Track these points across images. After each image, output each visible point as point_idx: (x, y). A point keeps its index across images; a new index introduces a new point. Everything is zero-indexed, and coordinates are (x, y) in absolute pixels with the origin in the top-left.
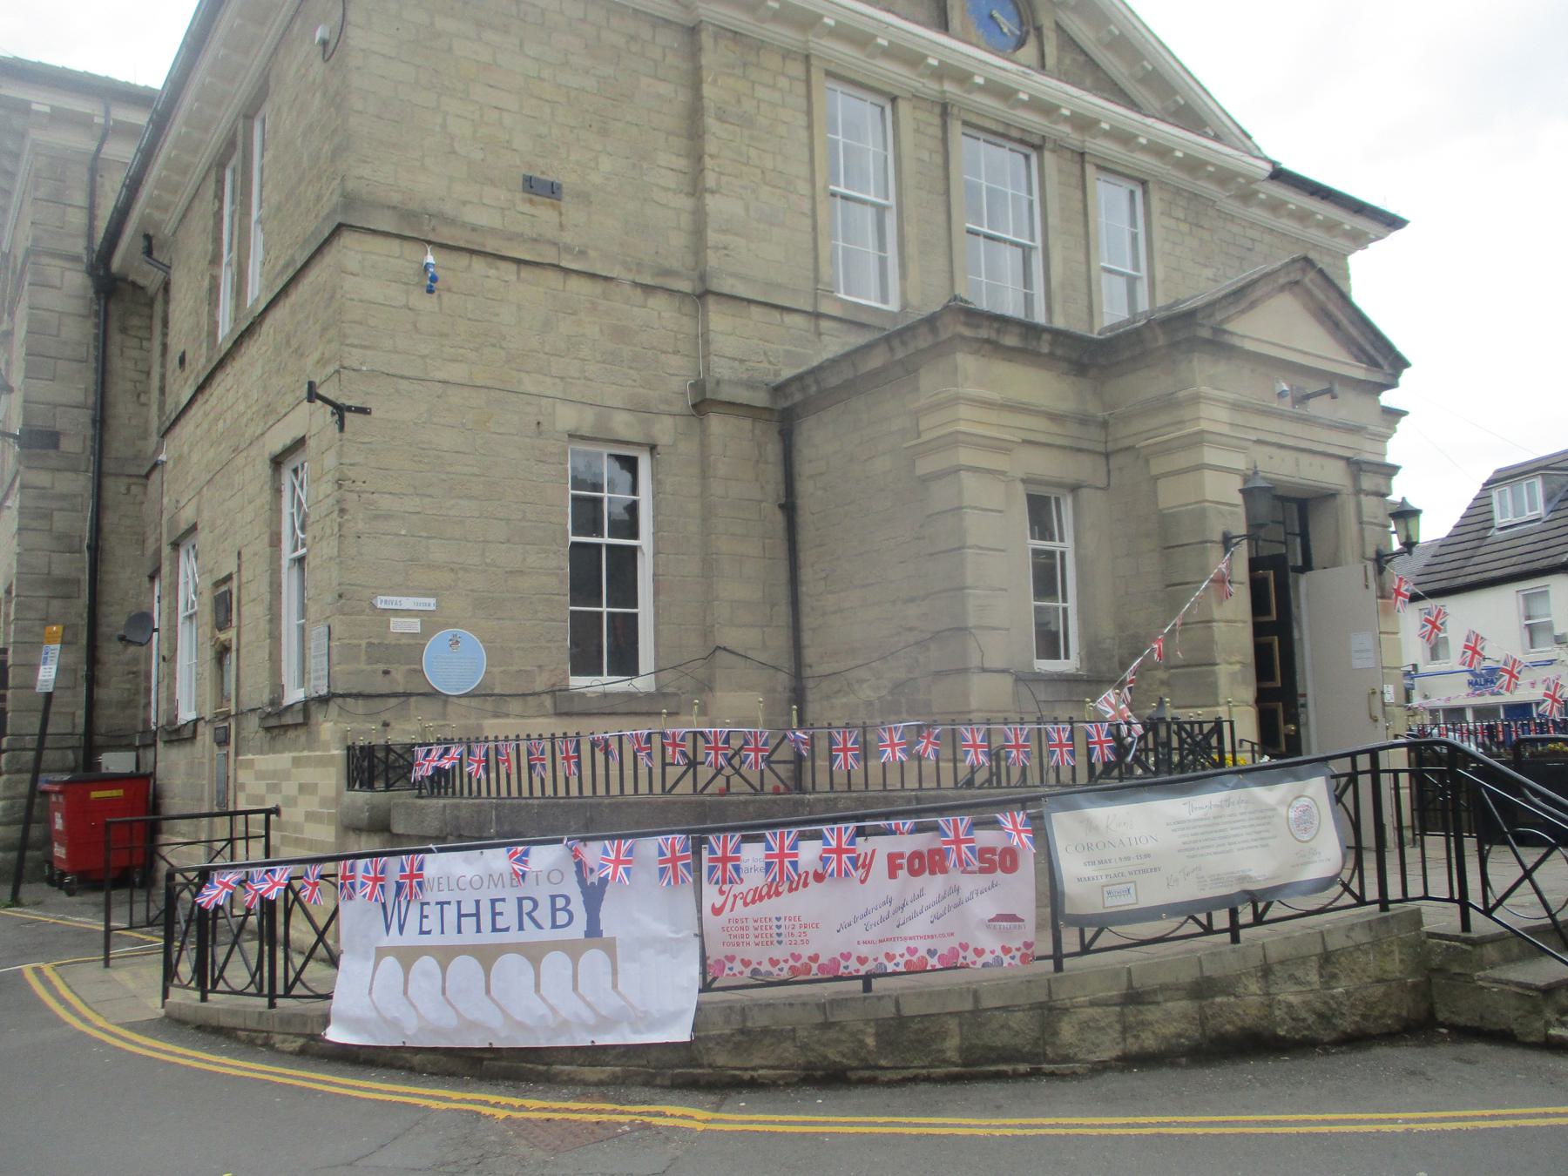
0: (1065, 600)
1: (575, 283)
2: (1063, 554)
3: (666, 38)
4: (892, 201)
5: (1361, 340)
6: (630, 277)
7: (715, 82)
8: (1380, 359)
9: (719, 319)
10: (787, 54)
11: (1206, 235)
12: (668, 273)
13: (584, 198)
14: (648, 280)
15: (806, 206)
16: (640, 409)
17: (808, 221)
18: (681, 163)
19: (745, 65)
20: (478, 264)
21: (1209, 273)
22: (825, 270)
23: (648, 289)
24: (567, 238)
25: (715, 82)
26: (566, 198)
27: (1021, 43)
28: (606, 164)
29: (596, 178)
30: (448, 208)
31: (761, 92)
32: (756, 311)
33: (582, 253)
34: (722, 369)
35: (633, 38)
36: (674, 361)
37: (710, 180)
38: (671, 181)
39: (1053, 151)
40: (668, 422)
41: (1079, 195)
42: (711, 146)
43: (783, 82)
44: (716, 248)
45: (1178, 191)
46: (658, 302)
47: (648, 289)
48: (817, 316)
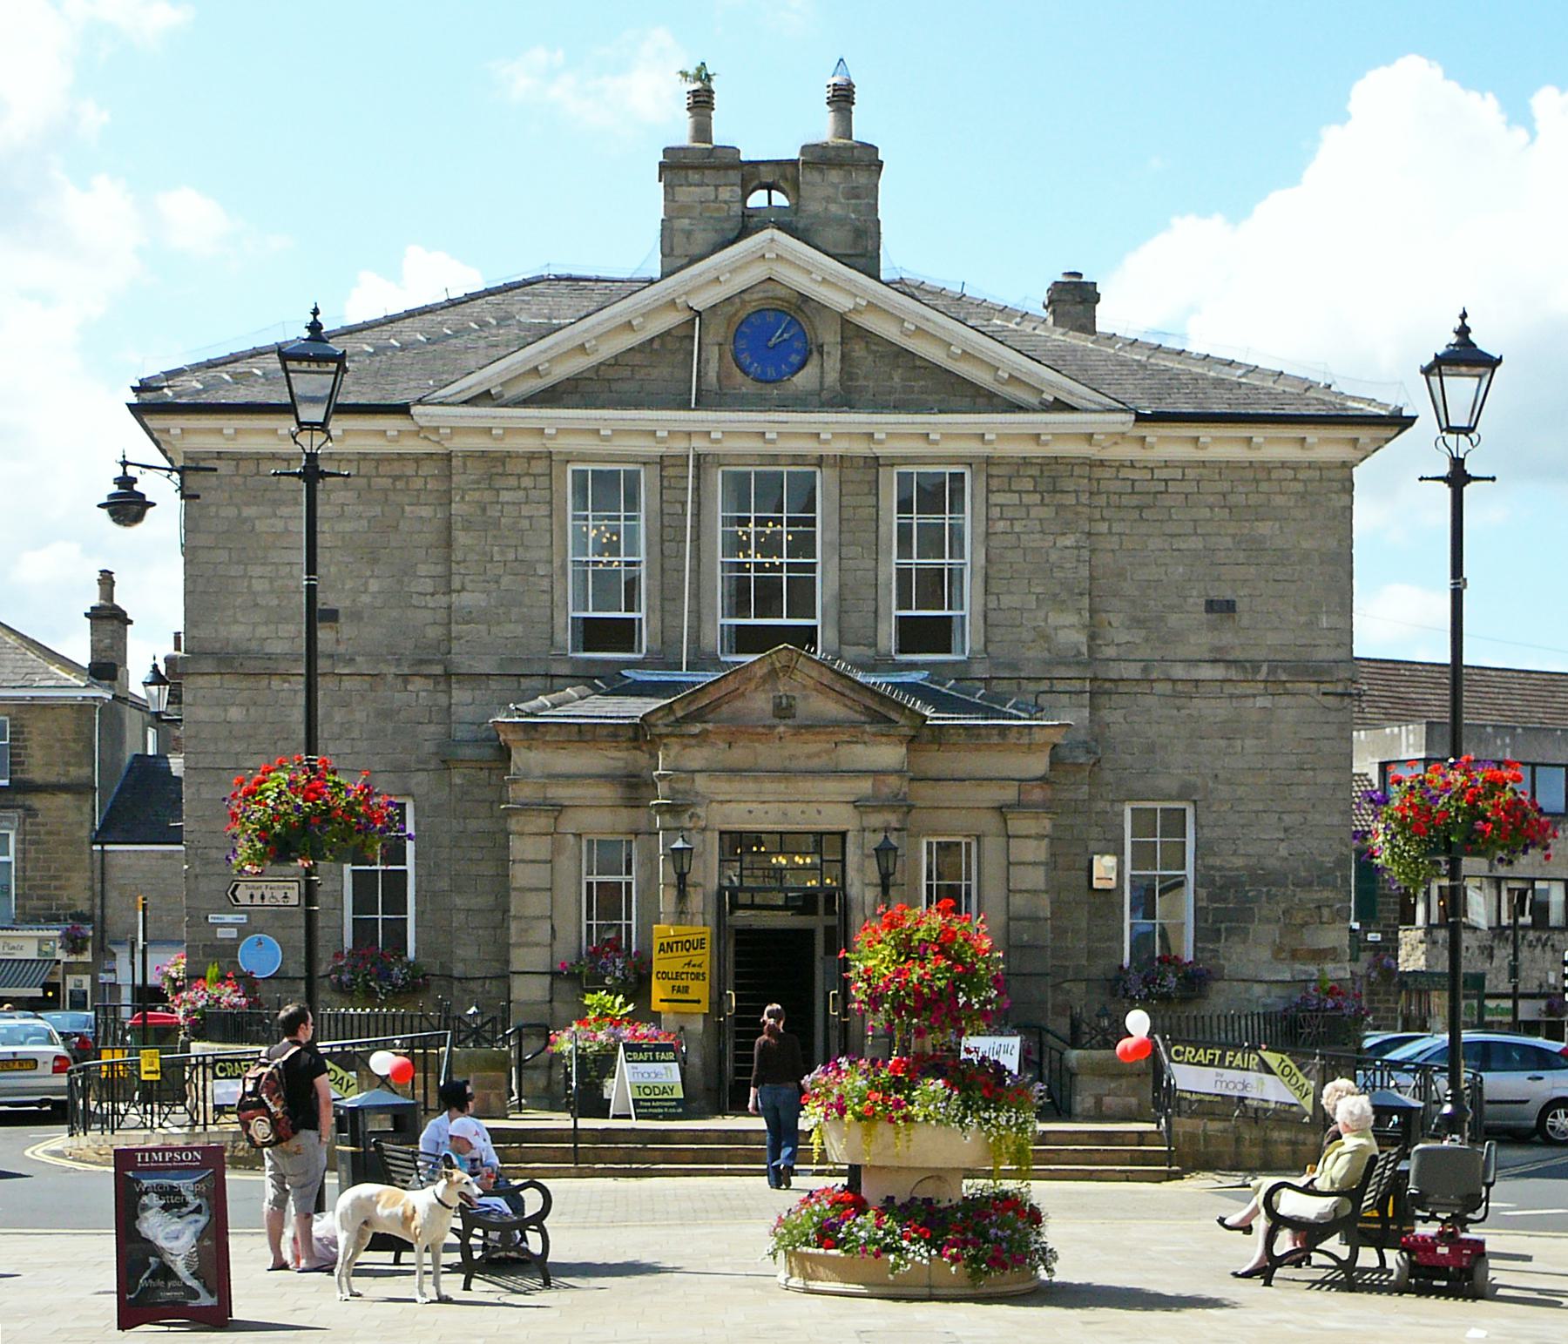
0: (629, 917)
1: (347, 684)
2: (629, 885)
3: (428, 468)
4: (643, 557)
5: (869, 702)
6: (393, 670)
7: (463, 498)
8: (894, 716)
9: (460, 695)
10: (531, 457)
11: (1070, 500)
12: (421, 662)
13: (356, 616)
14: (406, 671)
15: (545, 584)
16: (400, 769)
17: (547, 597)
18: (440, 569)
19: (491, 477)
20: (276, 683)
21: (1069, 541)
22: (558, 638)
23: (406, 678)
24: (342, 649)
25: (463, 498)
26: (342, 620)
27: (802, 365)
28: (374, 586)
29: (365, 599)
30: (254, 645)
31: (506, 496)
32: (493, 685)
33: (352, 660)
34: (461, 733)
35: (396, 478)
36: (432, 728)
37: (456, 585)
38: (428, 586)
39: (834, 465)
40: (421, 776)
41: (872, 500)
42: (458, 555)
43: (527, 482)
44: (459, 638)
45: (1026, 461)
46: (417, 684)
47: (406, 678)
48: (553, 676)
